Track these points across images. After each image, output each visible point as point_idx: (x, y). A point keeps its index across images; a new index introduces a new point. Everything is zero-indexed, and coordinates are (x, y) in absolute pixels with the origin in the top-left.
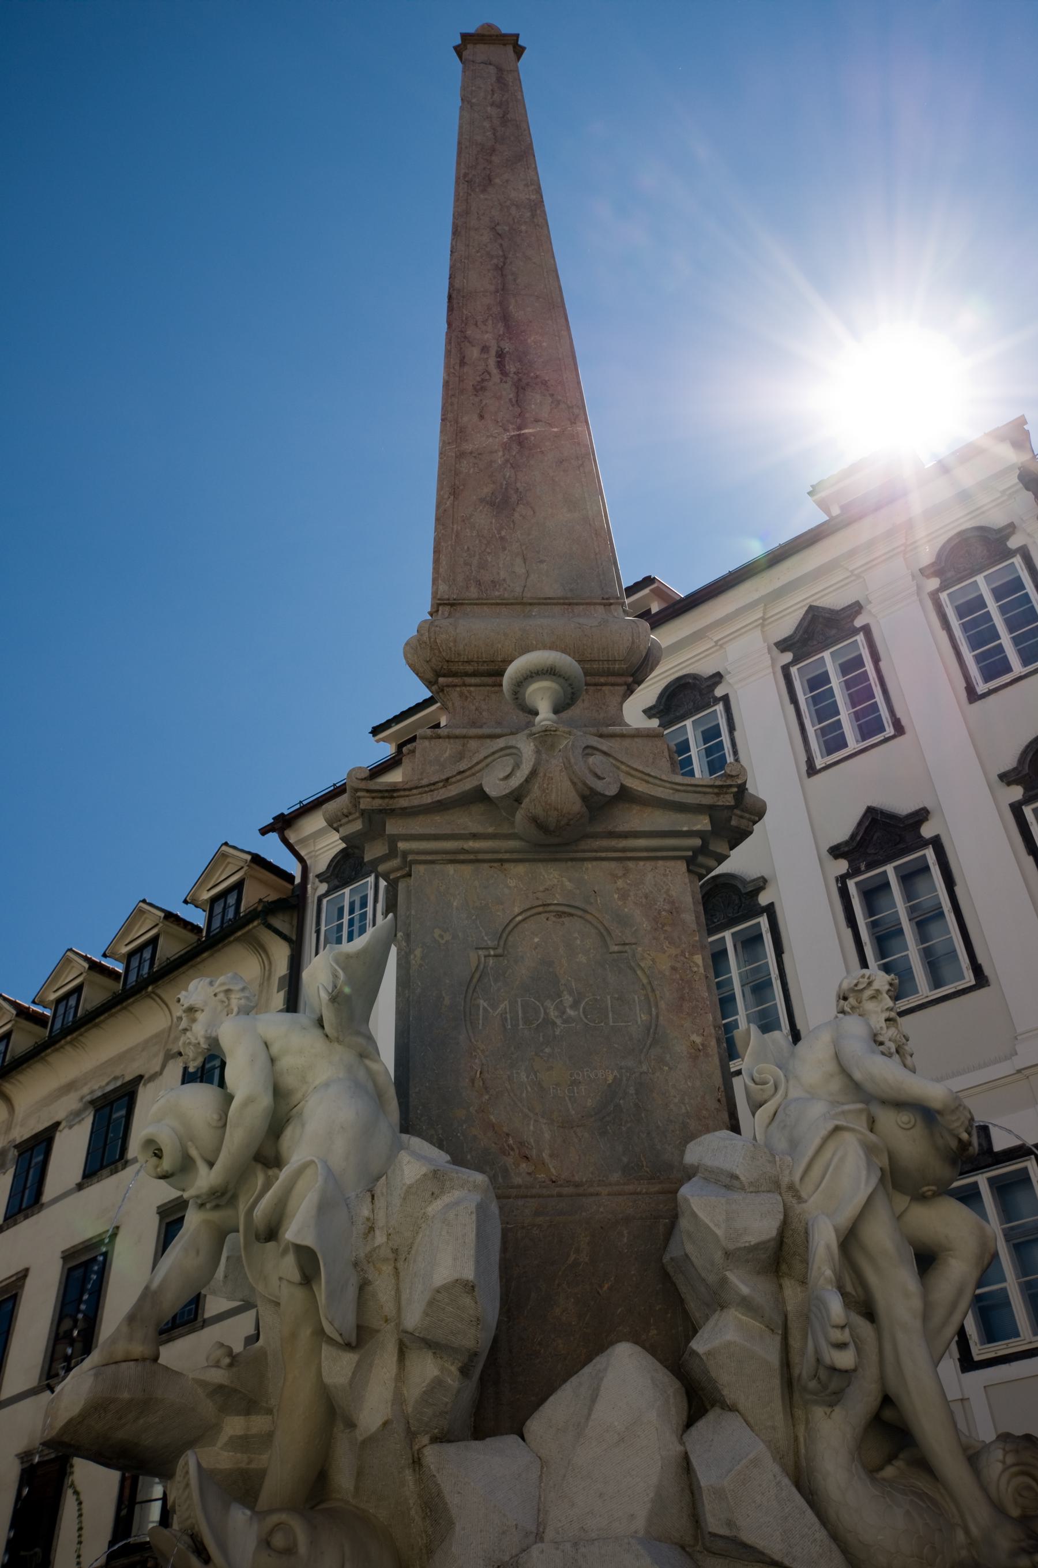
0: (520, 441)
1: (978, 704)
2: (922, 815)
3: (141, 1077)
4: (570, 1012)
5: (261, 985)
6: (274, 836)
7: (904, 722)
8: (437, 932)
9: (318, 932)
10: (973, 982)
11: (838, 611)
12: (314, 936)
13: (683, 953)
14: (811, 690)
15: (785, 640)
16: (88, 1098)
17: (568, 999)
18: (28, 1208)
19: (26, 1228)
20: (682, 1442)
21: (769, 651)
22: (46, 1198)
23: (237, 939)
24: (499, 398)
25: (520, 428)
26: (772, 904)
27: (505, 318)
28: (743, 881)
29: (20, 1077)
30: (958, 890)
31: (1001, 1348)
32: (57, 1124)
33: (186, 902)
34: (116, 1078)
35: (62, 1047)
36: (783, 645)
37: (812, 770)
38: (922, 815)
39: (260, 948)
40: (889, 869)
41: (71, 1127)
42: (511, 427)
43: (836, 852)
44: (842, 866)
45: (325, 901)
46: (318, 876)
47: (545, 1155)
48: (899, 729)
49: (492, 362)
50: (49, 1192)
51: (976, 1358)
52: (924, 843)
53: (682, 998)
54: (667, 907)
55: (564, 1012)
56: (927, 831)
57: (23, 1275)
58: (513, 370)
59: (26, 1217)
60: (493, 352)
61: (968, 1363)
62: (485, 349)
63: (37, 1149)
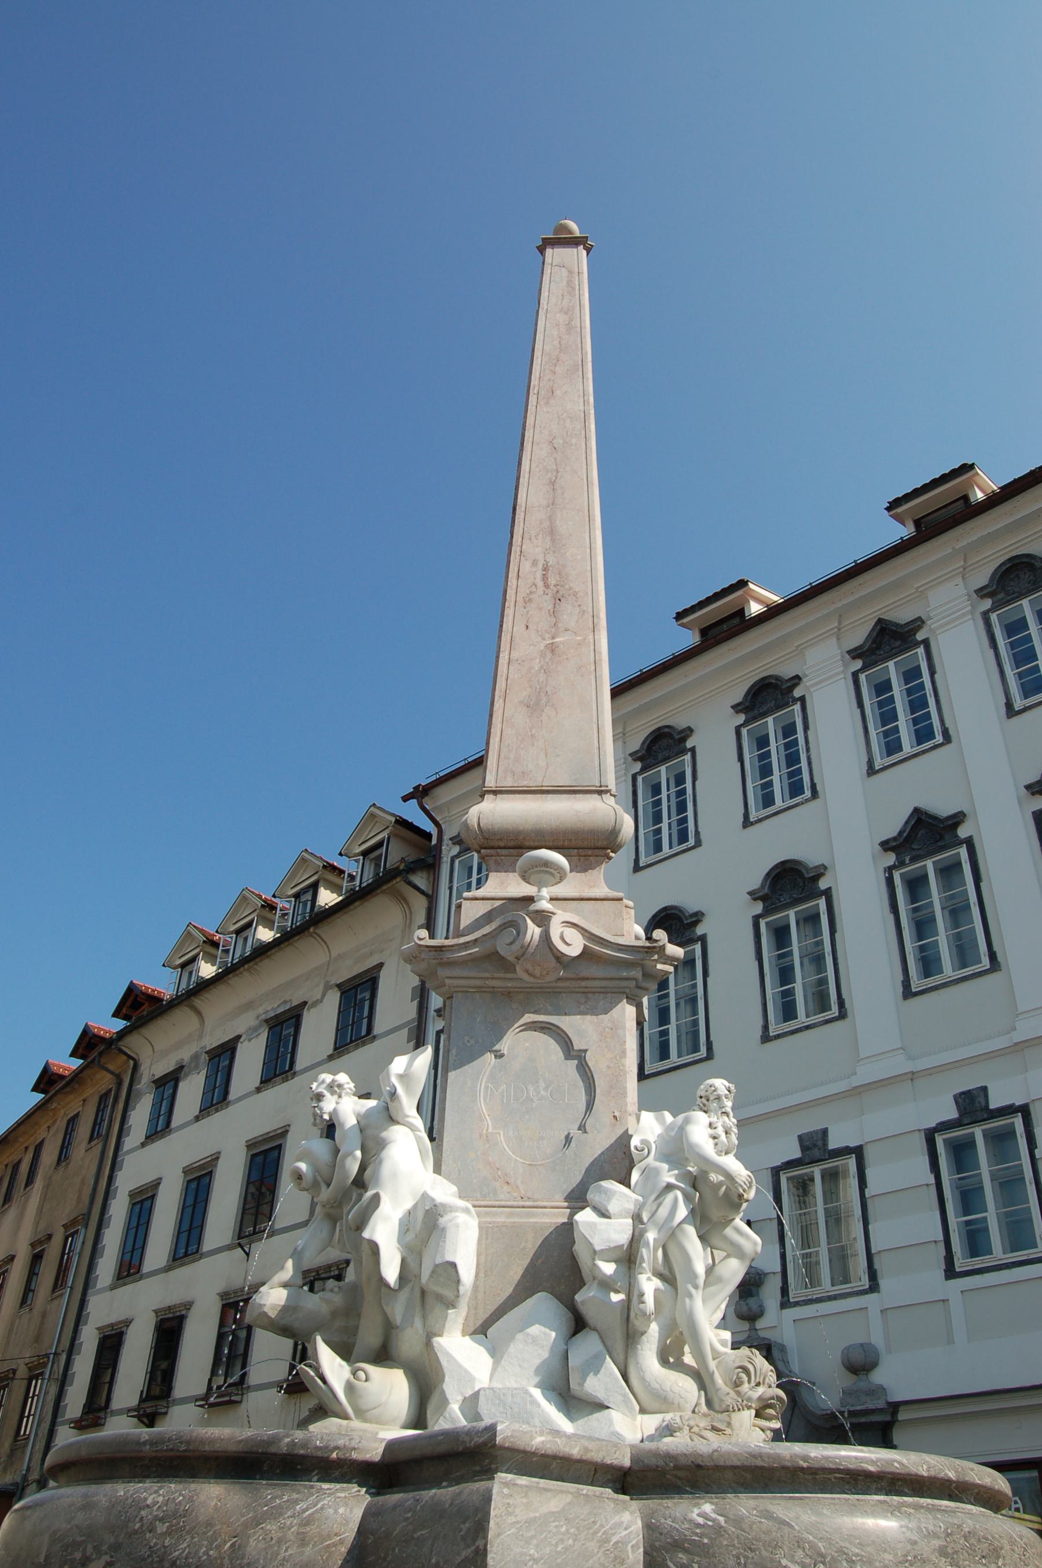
0: (552, 648)
1: (1016, 720)
2: (958, 819)
3: (305, 1003)
4: (543, 1093)
5: (403, 931)
6: (414, 802)
7: (951, 732)
8: (466, 1038)
9: (451, 888)
10: (988, 967)
11: (902, 626)
12: (448, 892)
13: (615, 1057)
14: (878, 695)
15: (856, 649)
16: (263, 1017)
17: (542, 1085)
18: (217, 1104)
19: (217, 1119)
20: (567, 1344)
21: (843, 657)
22: (232, 1096)
23: (383, 892)
24: (540, 609)
25: (553, 638)
26: (830, 888)
27: (552, 532)
28: (806, 867)
29: (207, 995)
30: (983, 885)
31: (978, 1262)
32: (239, 1037)
33: (340, 854)
34: (285, 1002)
35: (241, 973)
36: (855, 653)
37: (871, 771)
38: (958, 819)
39: (401, 899)
40: (929, 864)
41: (250, 1040)
42: (547, 636)
43: (886, 846)
44: (891, 859)
45: (457, 862)
46: (451, 839)
47: (519, 1182)
48: (947, 738)
49: (539, 575)
50: (233, 1094)
51: (957, 1270)
52: (960, 843)
53: (611, 1087)
54: (609, 1025)
55: (539, 1093)
56: (963, 832)
57: (215, 1158)
58: (554, 582)
59: (217, 1111)
60: (540, 566)
61: (951, 1272)
62: (535, 563)
63: (223, 1056)
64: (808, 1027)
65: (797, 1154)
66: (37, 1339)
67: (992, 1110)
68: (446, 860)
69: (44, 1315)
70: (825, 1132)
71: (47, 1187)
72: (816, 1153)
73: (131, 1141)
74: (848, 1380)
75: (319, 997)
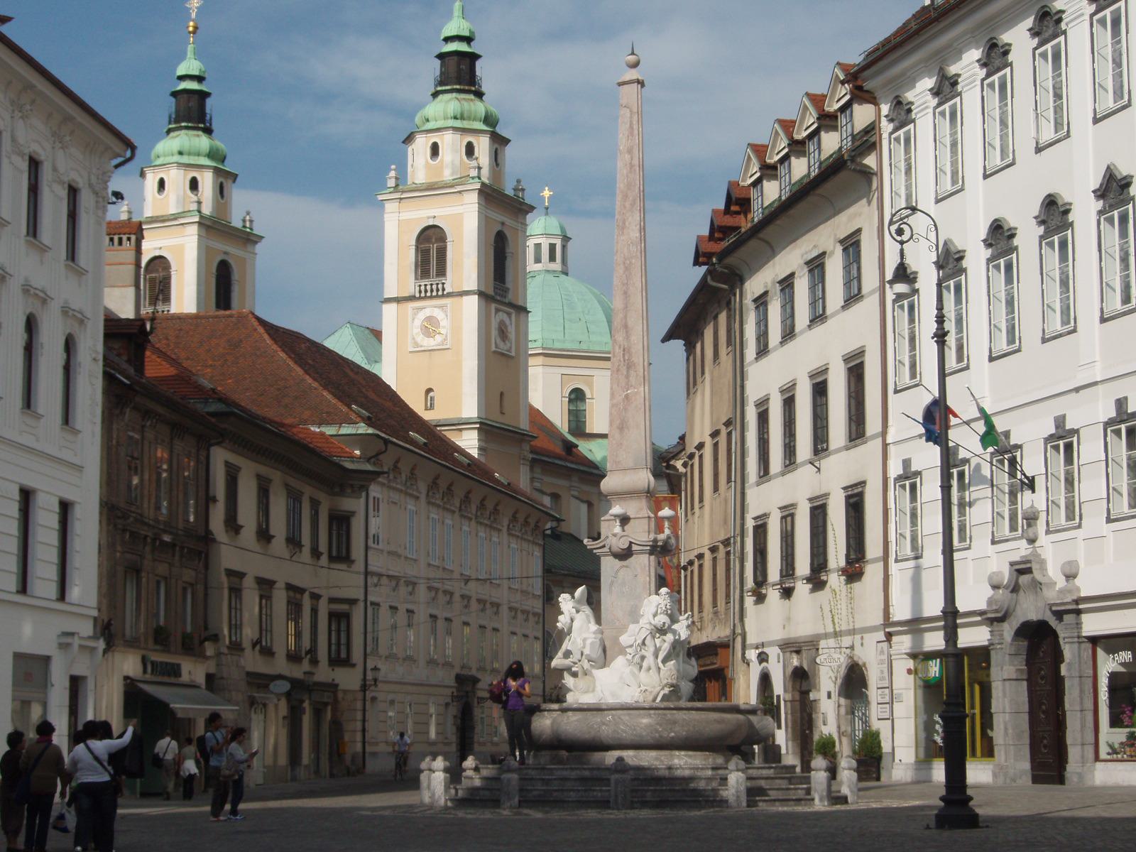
3: (824, 253)
27: (626, 326)
41: (800, 277)
62: (620, 348)
64: (1061, 336)
65: (1053, 431)
66: (725, 522)
67: (1129, 414)
68: (885, 136)
69: (726, 500)
70: (1064, 417)
71: (712, 380)
72: (1061, 433)
73: (751, 351)
74: (1061, 582)
75: (832, 248)
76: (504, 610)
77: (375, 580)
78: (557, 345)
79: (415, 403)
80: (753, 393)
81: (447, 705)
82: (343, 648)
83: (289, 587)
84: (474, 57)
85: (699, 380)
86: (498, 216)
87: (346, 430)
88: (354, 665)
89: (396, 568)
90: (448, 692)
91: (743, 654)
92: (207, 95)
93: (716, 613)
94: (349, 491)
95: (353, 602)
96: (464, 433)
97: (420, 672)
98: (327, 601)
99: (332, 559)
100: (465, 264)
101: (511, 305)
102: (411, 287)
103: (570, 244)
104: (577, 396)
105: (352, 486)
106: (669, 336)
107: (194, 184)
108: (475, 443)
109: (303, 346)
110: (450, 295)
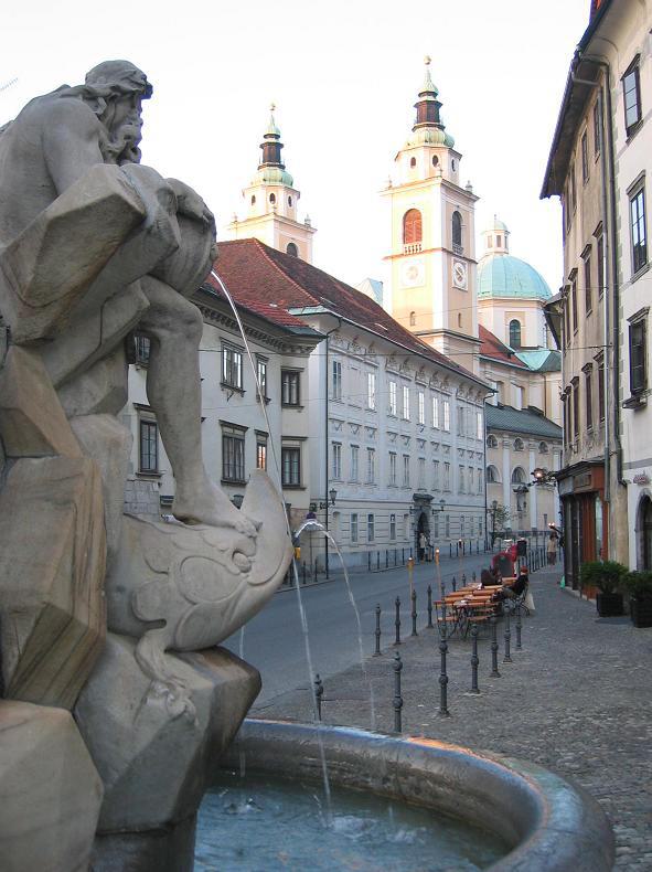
76: (453, 450)
77: (337, 424)
78: (502, 294)
79: (405, 323)
80: (624, 182)
81: (406, 515)
82: (295, 476)
83: (224, 424)
84: (439, 105)
85: (571, 218)
86: (455, 202)
87: (308, 311)
88: (304, 489)
89: (355, 417)
90: (408, 507)
91: (620, 475)
92: (281, 146)
93: (590, 434)
94: (299, 352)
95: (303, 439)
96: (435, 339)
97: (381, 493)
98: (280, 438)
99: (284, 405)
100: (435, 232)
101: (467, 259)
102: (401, 251)
103: (509, 237)
104: (515, 325)
105: (300, 347)
106: (546, 193)
107: (272, 198)
108: (442, 345)
109: (301, 267)
110: (425, 252)
